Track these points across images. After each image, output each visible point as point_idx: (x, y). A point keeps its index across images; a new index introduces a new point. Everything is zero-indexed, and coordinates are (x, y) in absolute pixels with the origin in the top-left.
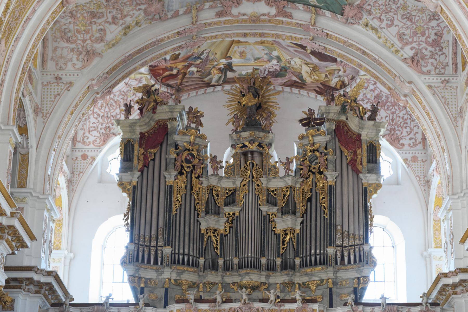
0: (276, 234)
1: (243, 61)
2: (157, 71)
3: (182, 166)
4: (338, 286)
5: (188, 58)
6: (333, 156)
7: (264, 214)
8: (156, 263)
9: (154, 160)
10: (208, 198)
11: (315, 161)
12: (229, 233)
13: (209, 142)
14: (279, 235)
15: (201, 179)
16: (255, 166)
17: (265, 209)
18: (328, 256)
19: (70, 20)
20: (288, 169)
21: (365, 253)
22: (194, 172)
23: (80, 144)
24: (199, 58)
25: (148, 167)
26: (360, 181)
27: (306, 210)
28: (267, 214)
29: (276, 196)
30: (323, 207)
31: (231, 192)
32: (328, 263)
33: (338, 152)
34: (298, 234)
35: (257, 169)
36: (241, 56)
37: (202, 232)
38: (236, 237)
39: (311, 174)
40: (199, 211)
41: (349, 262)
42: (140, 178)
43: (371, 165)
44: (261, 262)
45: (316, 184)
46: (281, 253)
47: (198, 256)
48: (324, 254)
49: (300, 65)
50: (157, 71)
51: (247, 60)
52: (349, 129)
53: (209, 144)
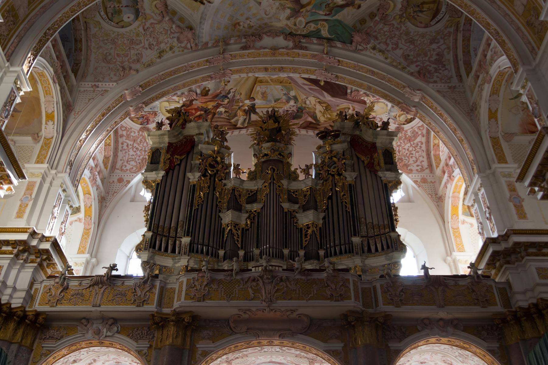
0: (298, 229)
1: (264, 102)
2: (190, 111)
3: (206, 170)
4: (367, 274)
5: (217, 96)
6: (350, 161)
7: (286, 210)
8: (173, 251)
9: (179, 165)
10: (230, 197)
11: (334, 166)
12: (251, 227)
13: (232, 152)
14: (301, 229)
15: (224, 181)
16: (276, 170)
17: (286, 206)
18: (354, 245)
19: (111, 46)
20: (308, 174)
21: (392, 240)
22: (217, 175)
23: (118, 170)
24: (226, 97)
25: (173, 170)
26: (378, 179)
27: (328, 206)
28: (288, 211)
29: (297, 196)
30: (344, 202)
31: (253, 193)
32: (354, 251)
33: (355, 158)
34: (320, 228)
35: (278, 174)
36: (263, 97)
37: (223, 226)
38: (258, 230)
39: (330, 176)
40: (221, 208)
41: (377, 250)
42: (165, 178)
43: (389, 166)
44: (283, 252)
45: (336, 184)
46: (304, 245)
47: (218, 247)
48: (349, 244)
49: (314, 105)
50: (190, 111)
51: (268, 101)
52: (364, 140)
53: (232, 155)
